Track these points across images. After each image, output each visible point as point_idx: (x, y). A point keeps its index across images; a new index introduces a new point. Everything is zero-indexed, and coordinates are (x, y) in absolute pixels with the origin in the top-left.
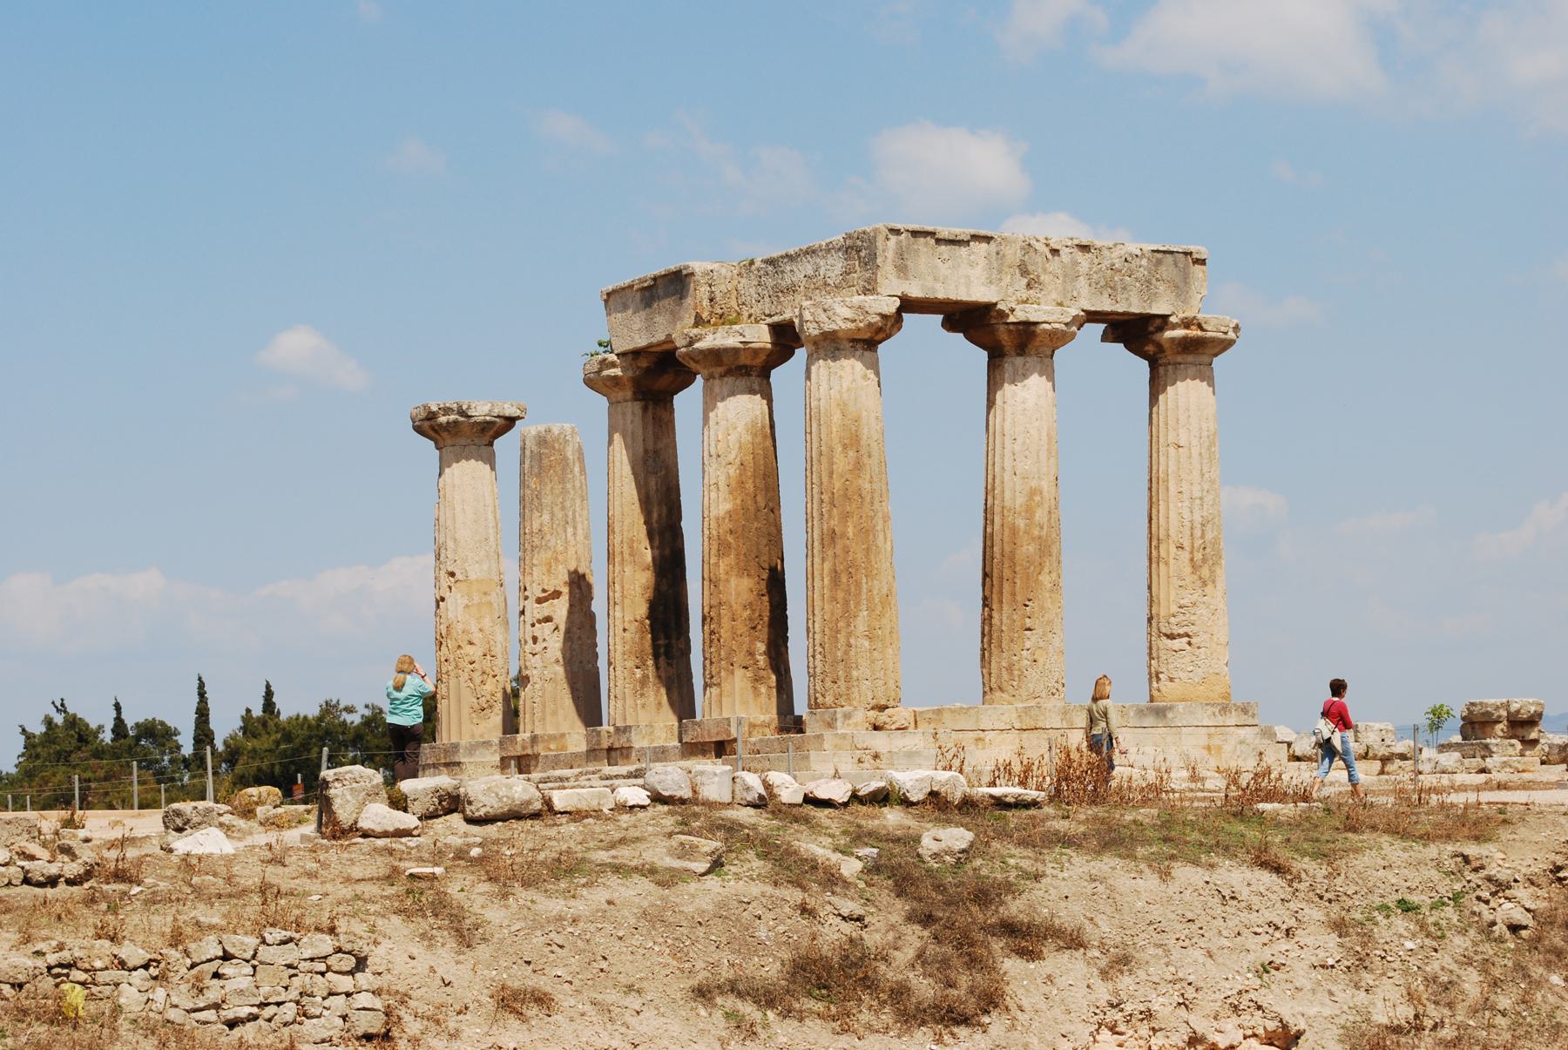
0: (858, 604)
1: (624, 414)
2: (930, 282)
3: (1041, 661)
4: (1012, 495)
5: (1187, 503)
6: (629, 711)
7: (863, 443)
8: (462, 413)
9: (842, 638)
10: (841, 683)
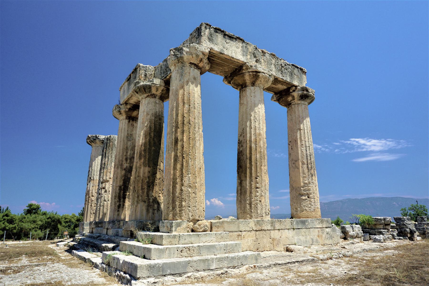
0: (187, 171)
1: (122, 123)
2: (221, 47)
3: (263, 201)
4: (251, 135)
5: (304, 148)
7: (192, 103)
9: (178, 186)
10: (178, 210)
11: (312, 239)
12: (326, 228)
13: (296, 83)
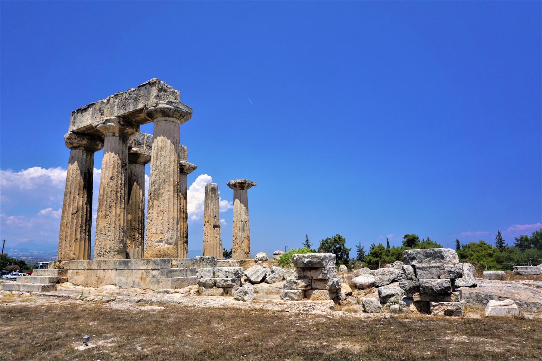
11: (134, 282)
12: (153, 270)
13: (140, 106)
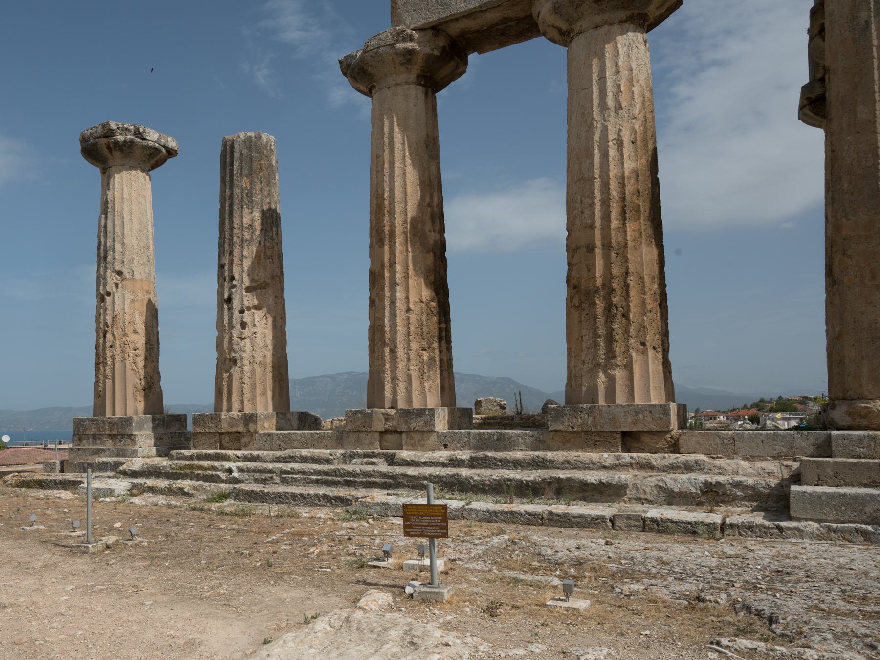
6: (416, 394)
8: (139, 134)
